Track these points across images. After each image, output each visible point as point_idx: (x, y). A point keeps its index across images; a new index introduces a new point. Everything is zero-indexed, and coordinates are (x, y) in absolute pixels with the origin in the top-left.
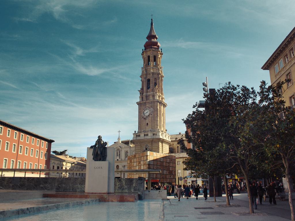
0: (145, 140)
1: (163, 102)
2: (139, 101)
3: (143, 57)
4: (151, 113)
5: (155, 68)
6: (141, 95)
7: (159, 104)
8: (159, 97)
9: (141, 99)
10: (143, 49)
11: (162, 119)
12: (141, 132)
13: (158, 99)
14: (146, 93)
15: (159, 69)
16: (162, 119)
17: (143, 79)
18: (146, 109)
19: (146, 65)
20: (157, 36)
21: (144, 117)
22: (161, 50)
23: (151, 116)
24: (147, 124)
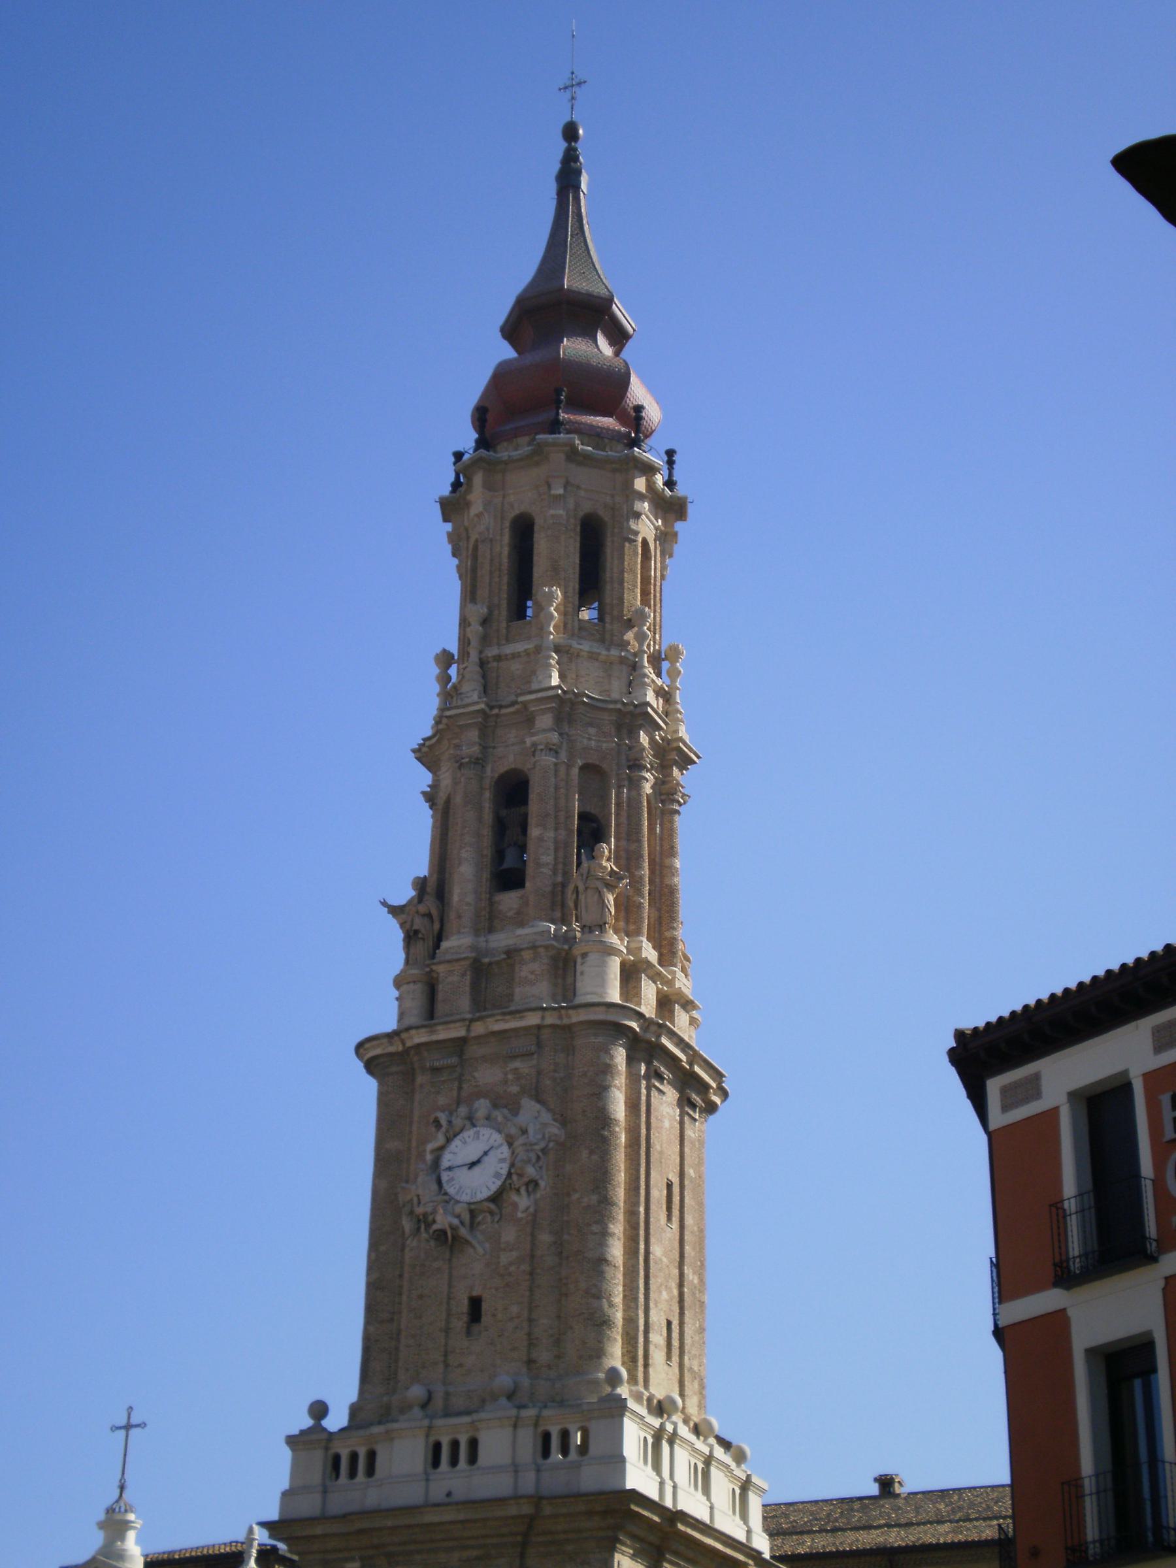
0: (431, 1517)
1: (672, 1034)
2: (390, 1024)
3: (457, 543)
4: (531, 1171)
5: (593, 657)
6: (420, 948)
7: (630, 1060)
8: (631, 974)
9: (416, 1004)
11: (657, 1250)
12: (385, 1415)
13: (614, 995)
14: (477, 932)
15: (635, 667)
16: (662, 1248)
17: (446, 780)
18: (471, 1120)
19: (485, 622)
20: (619, 310)
21: (443, 1220)
22: (671, 463)
23: (523, 1201)
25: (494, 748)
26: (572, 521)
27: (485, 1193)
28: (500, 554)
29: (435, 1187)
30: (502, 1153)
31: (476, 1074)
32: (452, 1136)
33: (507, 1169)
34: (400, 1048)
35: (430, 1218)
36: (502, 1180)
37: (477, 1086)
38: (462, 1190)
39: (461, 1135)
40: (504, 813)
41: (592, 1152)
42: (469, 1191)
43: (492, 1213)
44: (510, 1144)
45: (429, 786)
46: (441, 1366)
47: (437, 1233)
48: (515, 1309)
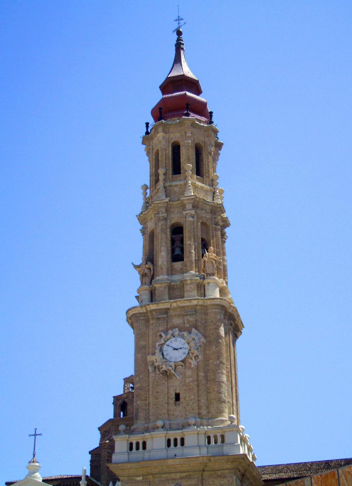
0: (170, 462)
6: (147, 280)
10: (147, 124)
21: (164, 368)
24: (178, 397)
25: (170, 215)
26: (193, 145)
27: (181, 359)
28: (168, 154)
29: (162, 356)
31: (172, 320)
32: (167, 340)
34: (145, 311)
35: (161, 367)
36: (186, 355)
40: (174, 236)
41: (216, 347)
42: (174, 358)
44: (188, 344)
45: (142, 228)
46: (167, 415)
48: (192, 397)
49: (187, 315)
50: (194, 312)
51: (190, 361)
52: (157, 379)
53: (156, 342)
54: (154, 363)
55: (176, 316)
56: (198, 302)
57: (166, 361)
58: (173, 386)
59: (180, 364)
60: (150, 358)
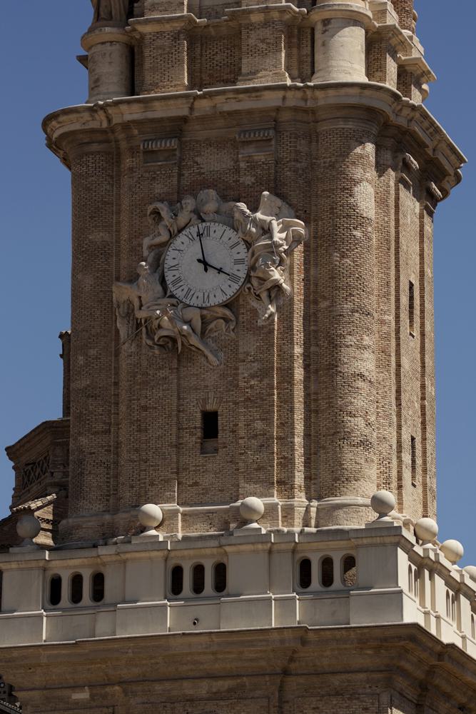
11: (405, 362)
24: (210, 424)
27: (221, 298)
29: (159, 288)
30: (238, 253)
31: (198, 159)
32: (176, 231)
33: (246, 272)
34: (105, 125)
35: (156, 323)
36: (240, 284)
37: (200, 174)
38: (192, 292)
39: (188, 230)
42: (201, 295)
43: (226, 320)
47: (161, 340)
49: (250, 142)
50: (272, 133)
51: (254, 304)
52: (145, 363)
53: (141, 235)
54: (133, 310)
55: (209, 143)
56: (284, 98)
57: (173, 305)
58: (196, 389)
59: (220, 315)
60: (122, 292)
